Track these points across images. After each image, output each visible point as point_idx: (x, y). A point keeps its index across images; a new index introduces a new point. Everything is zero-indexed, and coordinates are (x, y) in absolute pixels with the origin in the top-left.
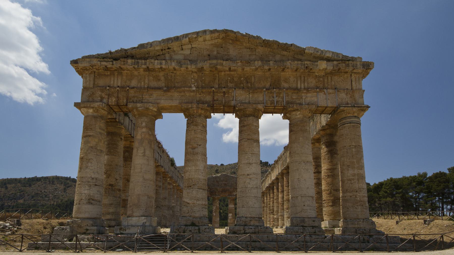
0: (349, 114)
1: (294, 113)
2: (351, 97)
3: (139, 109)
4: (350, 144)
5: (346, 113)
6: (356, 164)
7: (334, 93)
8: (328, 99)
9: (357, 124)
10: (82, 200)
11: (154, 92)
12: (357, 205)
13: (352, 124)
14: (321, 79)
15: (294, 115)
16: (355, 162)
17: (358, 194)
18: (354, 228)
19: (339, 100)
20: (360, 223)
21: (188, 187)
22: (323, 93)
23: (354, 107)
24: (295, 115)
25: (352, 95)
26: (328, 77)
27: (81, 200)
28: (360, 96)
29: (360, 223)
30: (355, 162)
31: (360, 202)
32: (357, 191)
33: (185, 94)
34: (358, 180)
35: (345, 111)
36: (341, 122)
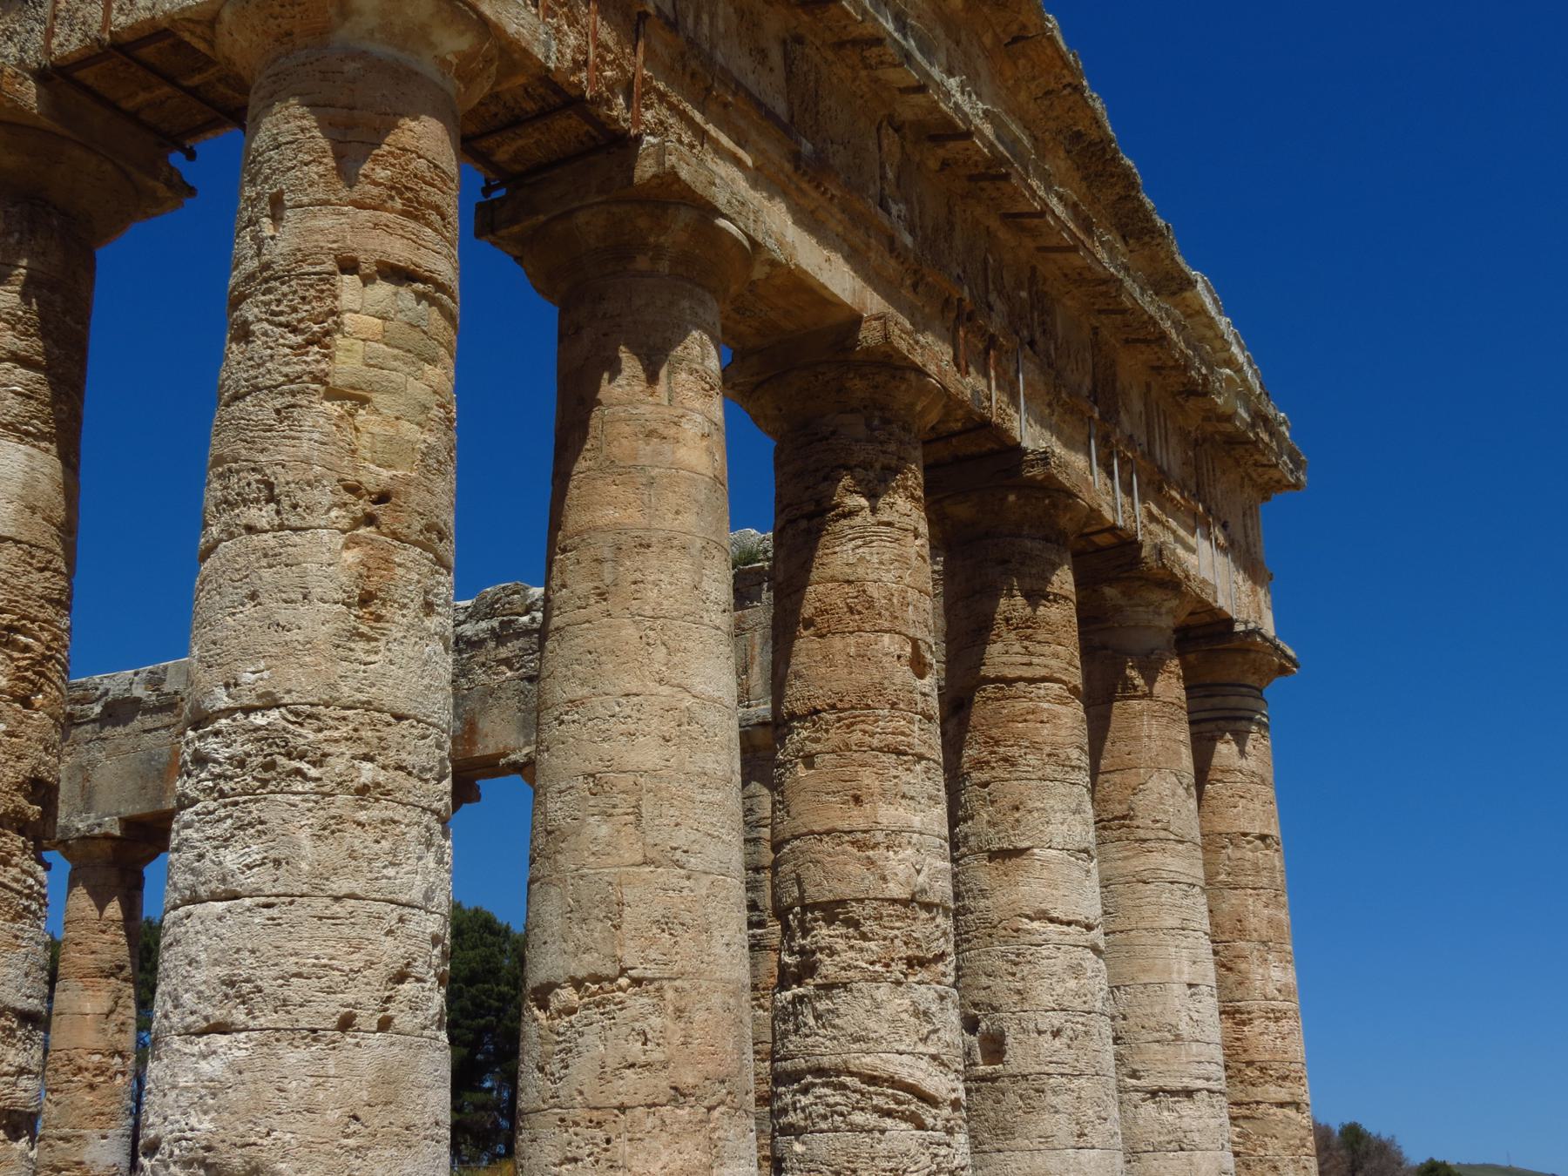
1: (1155, 596)
3: (723, 223)
4: (1266, 832)
5: (1246, 667)
10: (408, 987)
11: (754, 135)
15: (1149, 604)
21: (910, 962)
24: (1151, 608)
27: (401, 977)
33: (868, 246)
36: (1216, 701)
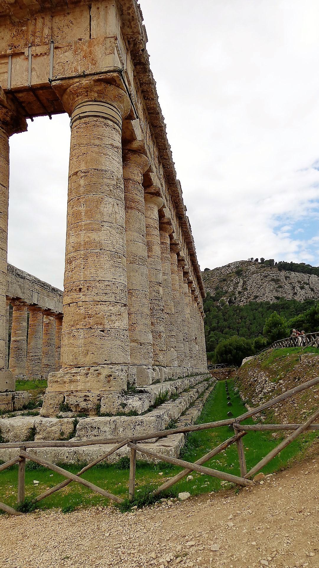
0: (78, 96)
2: (85, 57)
6: (84, 218)
7: (45, 54)
8: (32, 70)
9: (95, 119)
12: (78, 327)
13: (83, 120)
14: (24, 28)
16: (83, 214)
17: (83, 298)
18: (61, 393)
19: (57, 67)
20: (78, 378)
22: (22, 57)
23: (85, 76)
25: (88, 50)
26: (35, 19)
28: (106, 49)
29: (78, 378)
30: (83, 214)
31: (85, 318)
32: (80, 289)
34: (86, 258)
35: (68, 90)
